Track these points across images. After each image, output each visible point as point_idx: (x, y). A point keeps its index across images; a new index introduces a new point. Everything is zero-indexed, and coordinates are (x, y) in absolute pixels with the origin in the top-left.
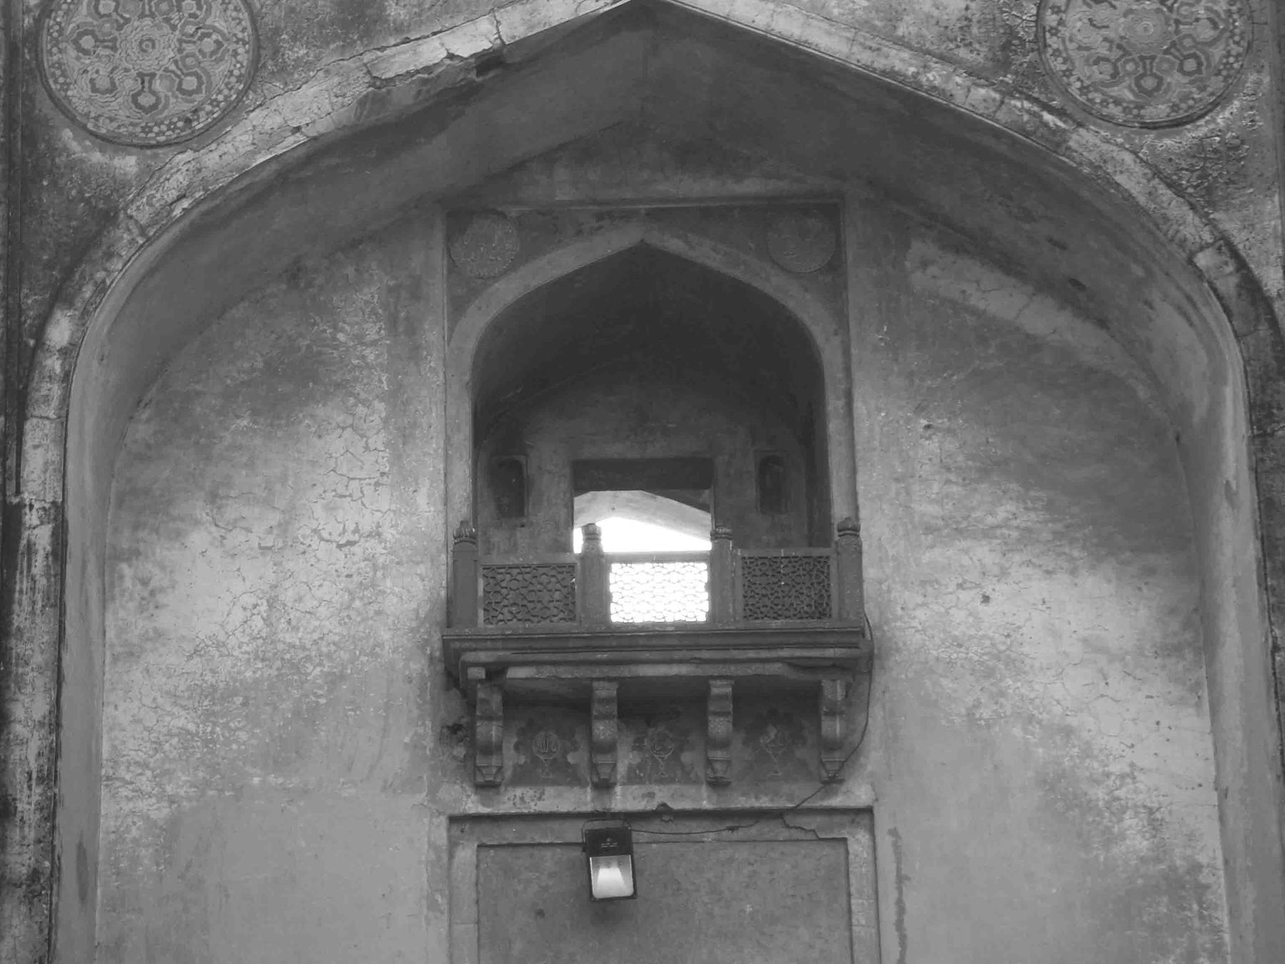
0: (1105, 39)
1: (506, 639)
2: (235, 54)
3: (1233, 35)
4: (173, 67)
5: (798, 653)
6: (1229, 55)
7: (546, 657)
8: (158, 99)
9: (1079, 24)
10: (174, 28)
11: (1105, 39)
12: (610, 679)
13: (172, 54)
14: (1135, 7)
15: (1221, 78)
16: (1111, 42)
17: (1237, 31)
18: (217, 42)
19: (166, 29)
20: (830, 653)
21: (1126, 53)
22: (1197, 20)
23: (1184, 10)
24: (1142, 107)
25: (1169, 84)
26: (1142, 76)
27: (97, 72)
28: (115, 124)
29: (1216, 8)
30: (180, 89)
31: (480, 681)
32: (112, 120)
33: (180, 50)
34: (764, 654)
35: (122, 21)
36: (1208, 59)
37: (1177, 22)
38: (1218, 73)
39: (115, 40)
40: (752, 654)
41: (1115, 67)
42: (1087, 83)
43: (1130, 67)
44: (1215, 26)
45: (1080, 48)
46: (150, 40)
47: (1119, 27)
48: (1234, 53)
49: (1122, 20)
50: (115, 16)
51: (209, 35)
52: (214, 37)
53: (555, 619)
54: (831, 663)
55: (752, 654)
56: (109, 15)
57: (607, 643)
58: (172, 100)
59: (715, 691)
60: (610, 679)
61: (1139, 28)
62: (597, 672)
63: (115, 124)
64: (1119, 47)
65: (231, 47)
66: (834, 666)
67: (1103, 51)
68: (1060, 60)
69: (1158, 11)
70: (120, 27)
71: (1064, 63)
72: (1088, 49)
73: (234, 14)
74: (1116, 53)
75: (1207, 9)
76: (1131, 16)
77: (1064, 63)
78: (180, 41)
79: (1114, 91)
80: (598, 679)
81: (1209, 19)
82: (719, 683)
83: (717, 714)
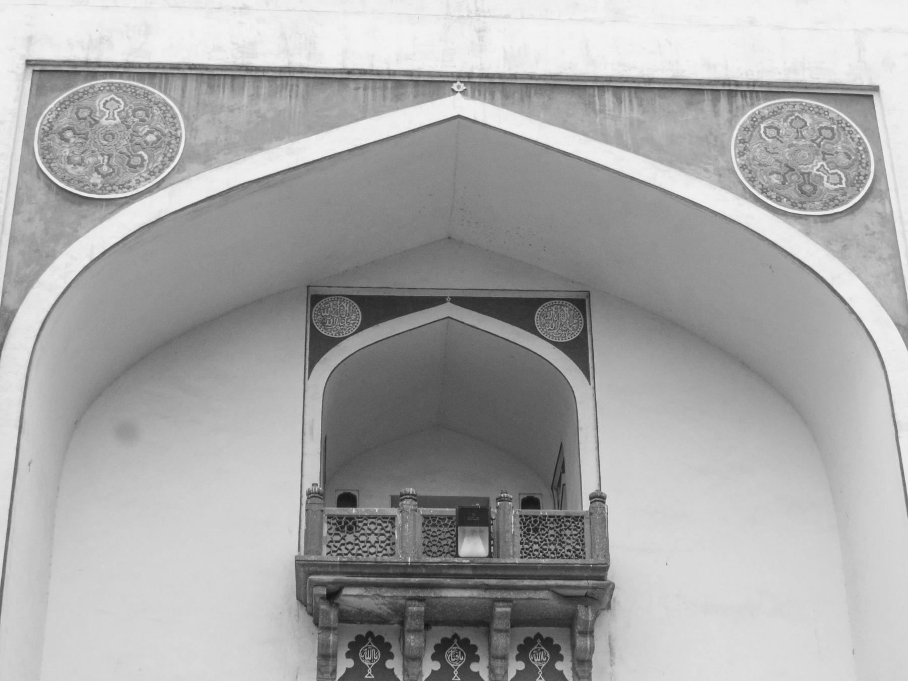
0: (776, 161)
1: (343, 564)
2: (169, 144)
3: (861, 163)
4: (125, 150)
5: (560, 582)
6: (859, 175)
7: (372, 579)
8: (114, 171)
9: (758, 150)
10: (128, 127)
11: (776, 161)
12: (421, 600)
13: (125, 143)
14: (795, 142)
15: (855, 188)
16: (781, 163)
17: (864, 161)
18: (156, 136)
19: (123, 127)
20: (583, 583)
21: (792, 170)
22: (837, 153)
23: (827, 146)
24: (804, 203)
25: (821, 190)
26: (804, 183)
27: (73, 152)
28: (82, 185)
29: (848, 146)
30: (128, 164)
31: (322, 598)
32: (79, 182)
33: (131, 141)
34: (535, 583)
35: (93, 122)
36: (846, 176)
37: (824, 153)
38: (853, 185)
39: (87, 134)
40: (527, 582)
41: (784, 176)
42: (766, 185)
43: (794, 177)
44: (850, 158)
45: (760, 165)
46: (111, 134)
47: (785, 154)
48: (862, 173)
49: (787, 149)
50: (89, 119)
51: (151, 132)
52: (156, 133)
53: (380, 555)
54: (582, 592)
55: (527, 582)
56: (85, 119)
57: (418, 571)
58: (122, 171)
59: (500, 609)
60: (421, 600)
61: (799, 155)
62: (410, 593)
63: (82, 185)
64: (787, 166)
65: (167, 140)
66: (586, 596)
67: (776, 167)
68: (747, 171)
69: (810, 146)
70: (91, 125)
71: (750, 173)
72: (766, 166)
73: (171, 120)
74: (785, 169)
75: (843, 147)
76: (793, 148)
77: (750, 173)
78: (132, 135)
79: (783, 192)
80: (411, 599)
81: (845, 153)
82: (501, 604)
83: (500, 631)
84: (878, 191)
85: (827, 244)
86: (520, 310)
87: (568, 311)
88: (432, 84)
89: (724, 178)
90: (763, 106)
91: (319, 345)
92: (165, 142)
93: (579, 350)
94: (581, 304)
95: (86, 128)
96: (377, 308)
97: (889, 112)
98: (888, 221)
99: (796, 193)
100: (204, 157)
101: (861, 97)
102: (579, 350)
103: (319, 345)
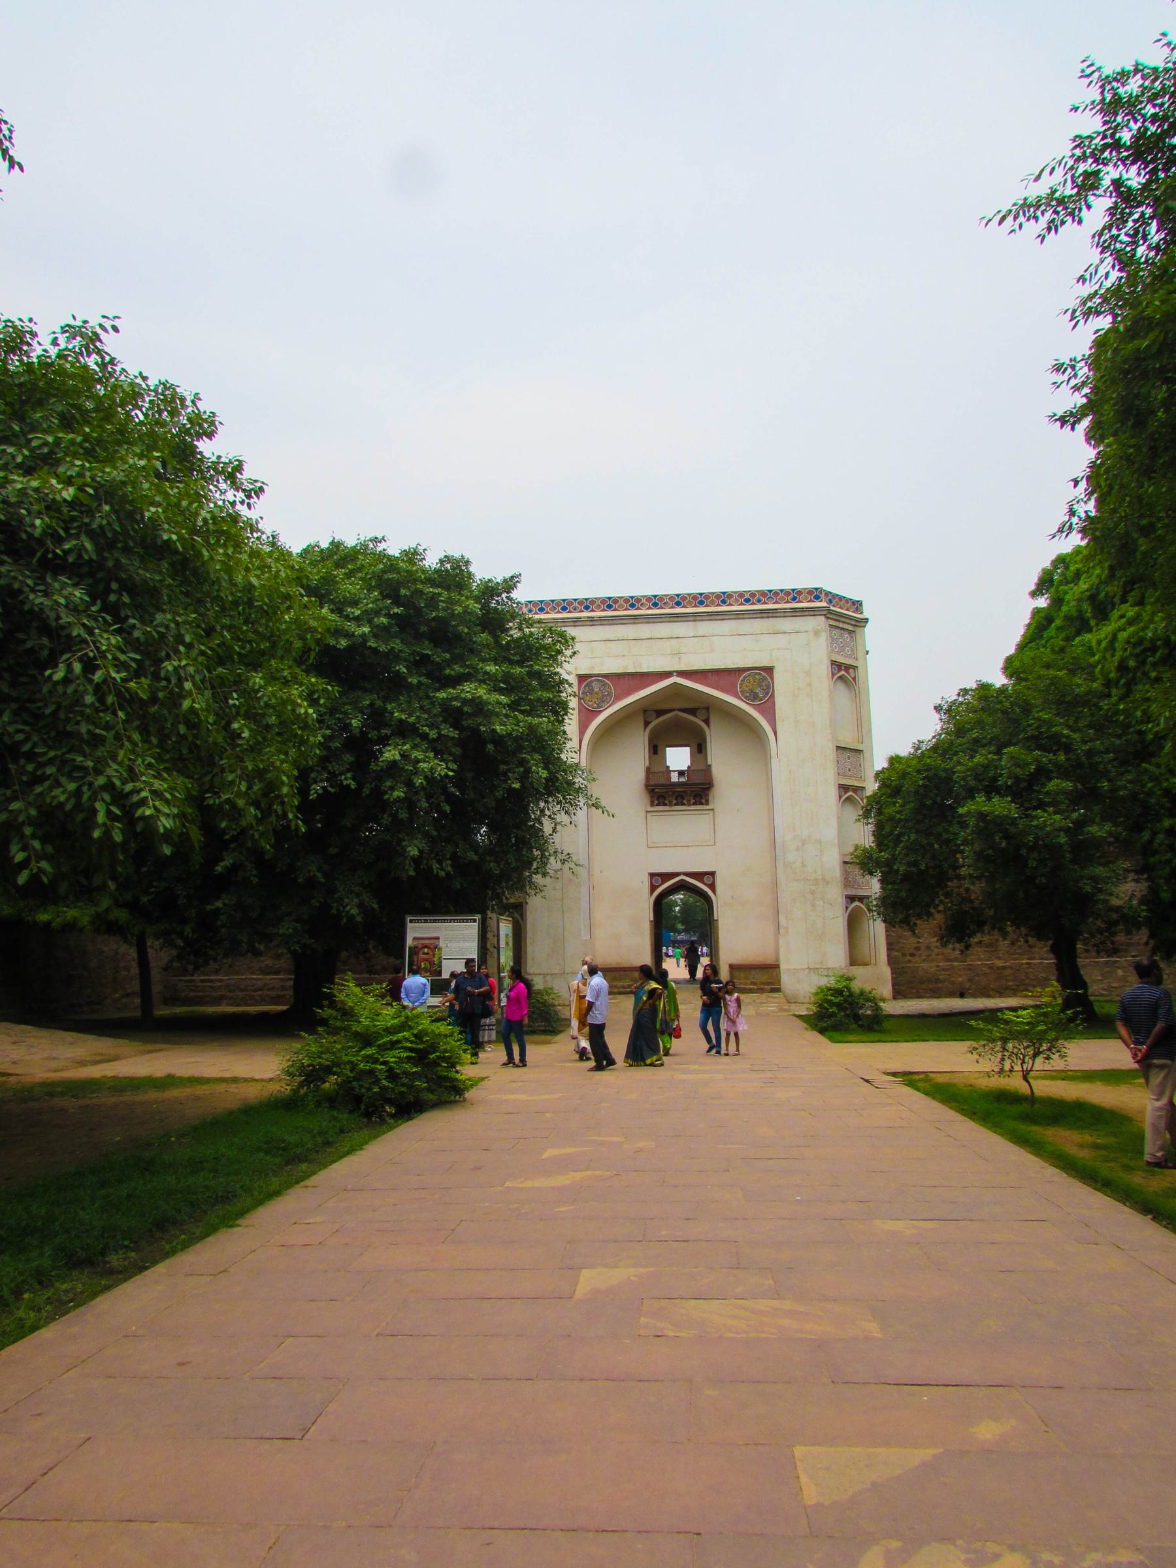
84: (772, 696)
85: (759, 711)
86: (693, 711)
87: (704, 711)
88: (668, 674)
89: (736, 695)
90: (745, 674)
91: (647, 724)
92: (610, 694)
93: (707, 722)
94: (707, 709)
95: (591, 692)
96: (660, 713)
97: (777, 674)
98: (774, 703)
99: (751, 697)
100: (618, 698)
101: (769, 670)
102: (707, 722)
103: (647, 724)
